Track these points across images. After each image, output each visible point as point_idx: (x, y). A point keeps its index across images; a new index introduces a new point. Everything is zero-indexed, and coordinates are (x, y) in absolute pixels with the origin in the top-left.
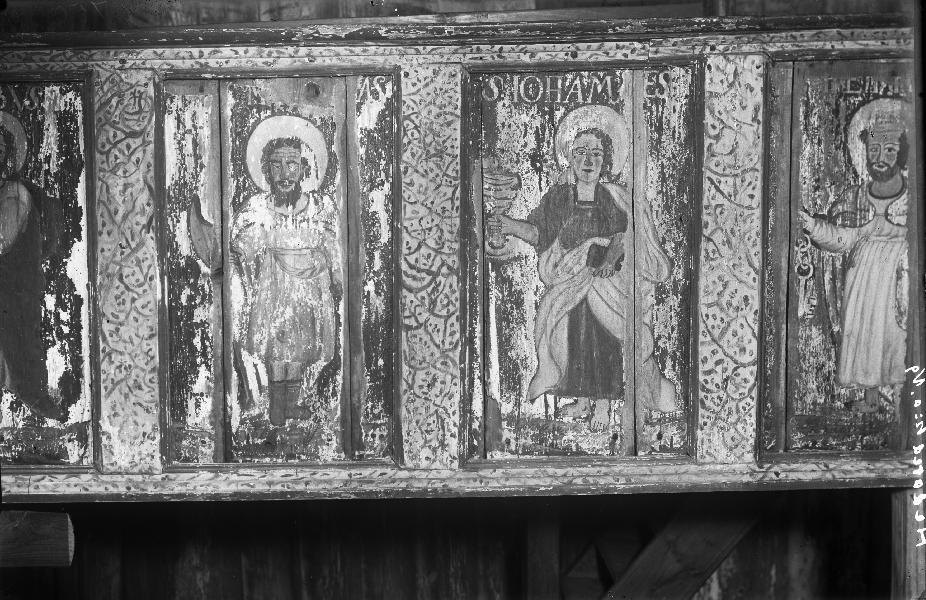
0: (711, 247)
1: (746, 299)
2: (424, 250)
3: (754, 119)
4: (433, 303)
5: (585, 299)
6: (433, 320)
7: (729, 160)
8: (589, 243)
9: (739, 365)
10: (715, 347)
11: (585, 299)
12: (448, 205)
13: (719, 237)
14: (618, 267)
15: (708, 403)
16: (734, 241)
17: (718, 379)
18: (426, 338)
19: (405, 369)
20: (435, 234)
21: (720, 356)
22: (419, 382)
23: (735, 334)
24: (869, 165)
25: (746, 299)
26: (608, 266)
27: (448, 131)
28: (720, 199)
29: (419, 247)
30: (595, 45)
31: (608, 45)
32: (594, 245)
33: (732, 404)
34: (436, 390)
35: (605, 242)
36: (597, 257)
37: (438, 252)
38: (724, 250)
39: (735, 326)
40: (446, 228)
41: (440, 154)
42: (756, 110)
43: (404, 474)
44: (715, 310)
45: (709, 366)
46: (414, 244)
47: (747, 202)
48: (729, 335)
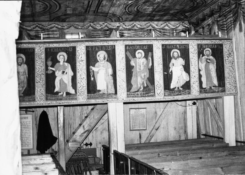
0: (79, 71)
1: (84, 78)
2: (39, 72)
3: (84, 53)
4: (41, 79)
5: (62, 78)
6: (41, 81)
7: (81, 59)
8: (62, 71)
9: (83, 87)
10: (80, 84)
11: (62, 78)
12: (42, 65)
13: (80, 69)
14: (66, 74)
15: (79, 92)
16: (82, 70)
17: (80, 88)
18: (40, 84)
19: (37, 88)
20: (41, 69)
21: (81, 86)
22: (39, 90)
23: (82, 82)
24: (100, 59)
25: (84, 78)
26: (65, 73)
27: (42, 55)
28: (80, 64)
29: (38, 71)
30: (62, 44)
31: (64, 44)
32: (63, 71)
33: (83, 92)
34: (41, 91)
35: (64, 70)
36: (63, 72)
37: (41, 72)
38: (81, 71)
39: (82, 81)
40: (42, 68)
41: (41, 58)
42: (84, 52)
43: (37, 103)
44: (80, 79)
45: (79, 87)
46: (38, 71)
47: (83, 65)
48: (82, 82)
